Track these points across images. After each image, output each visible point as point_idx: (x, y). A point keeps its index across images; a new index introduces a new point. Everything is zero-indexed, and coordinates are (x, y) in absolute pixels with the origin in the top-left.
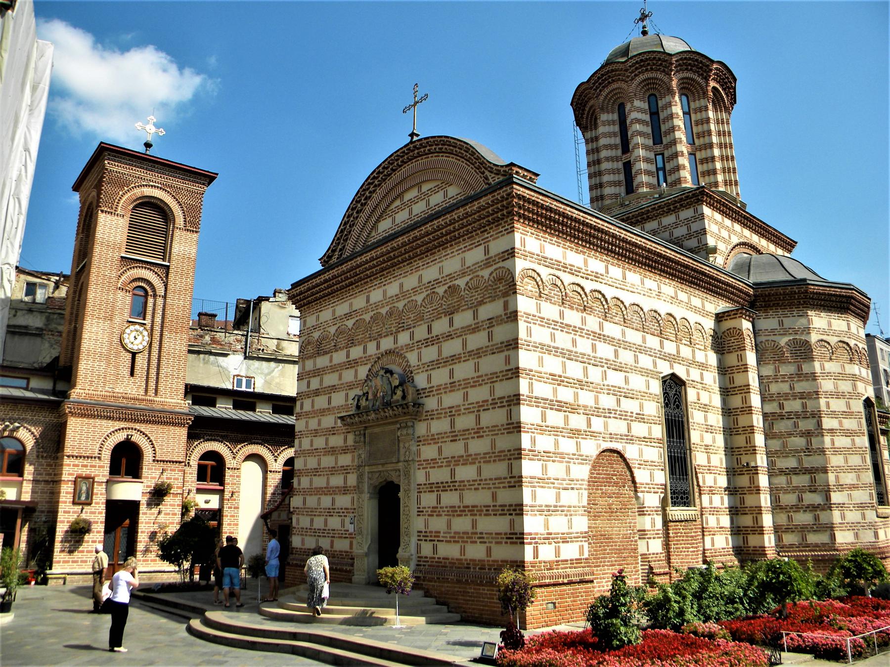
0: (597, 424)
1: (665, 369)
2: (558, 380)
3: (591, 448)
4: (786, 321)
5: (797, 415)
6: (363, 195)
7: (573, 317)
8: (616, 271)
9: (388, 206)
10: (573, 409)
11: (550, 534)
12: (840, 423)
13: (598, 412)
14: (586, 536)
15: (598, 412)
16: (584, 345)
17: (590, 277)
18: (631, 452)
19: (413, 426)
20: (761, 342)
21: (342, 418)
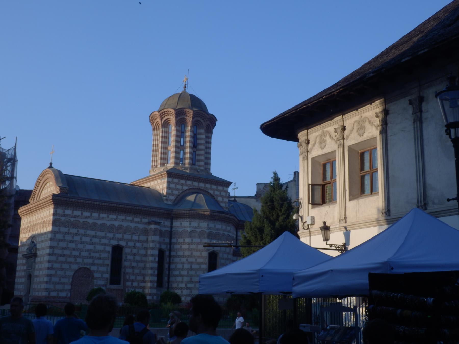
0: (79, 260)
1: (115, 243)
2: (63, 248)
3: (75, 267)
4: (182, 223)
5: (181, 256)
6: (38, 181)
7: (73, 231)
8: (95, 215)
9: (44, 186)
10: (70, 256)
11: (56, 289)
12: (196, 260)
13: (80, 257)
14: (70, 291)
15: (80, 257)
16: (77, 238)
17: (83, 218)
18: (93, 268)
19: (35, 259)
20: (174, 231)
21: (23, 255)
